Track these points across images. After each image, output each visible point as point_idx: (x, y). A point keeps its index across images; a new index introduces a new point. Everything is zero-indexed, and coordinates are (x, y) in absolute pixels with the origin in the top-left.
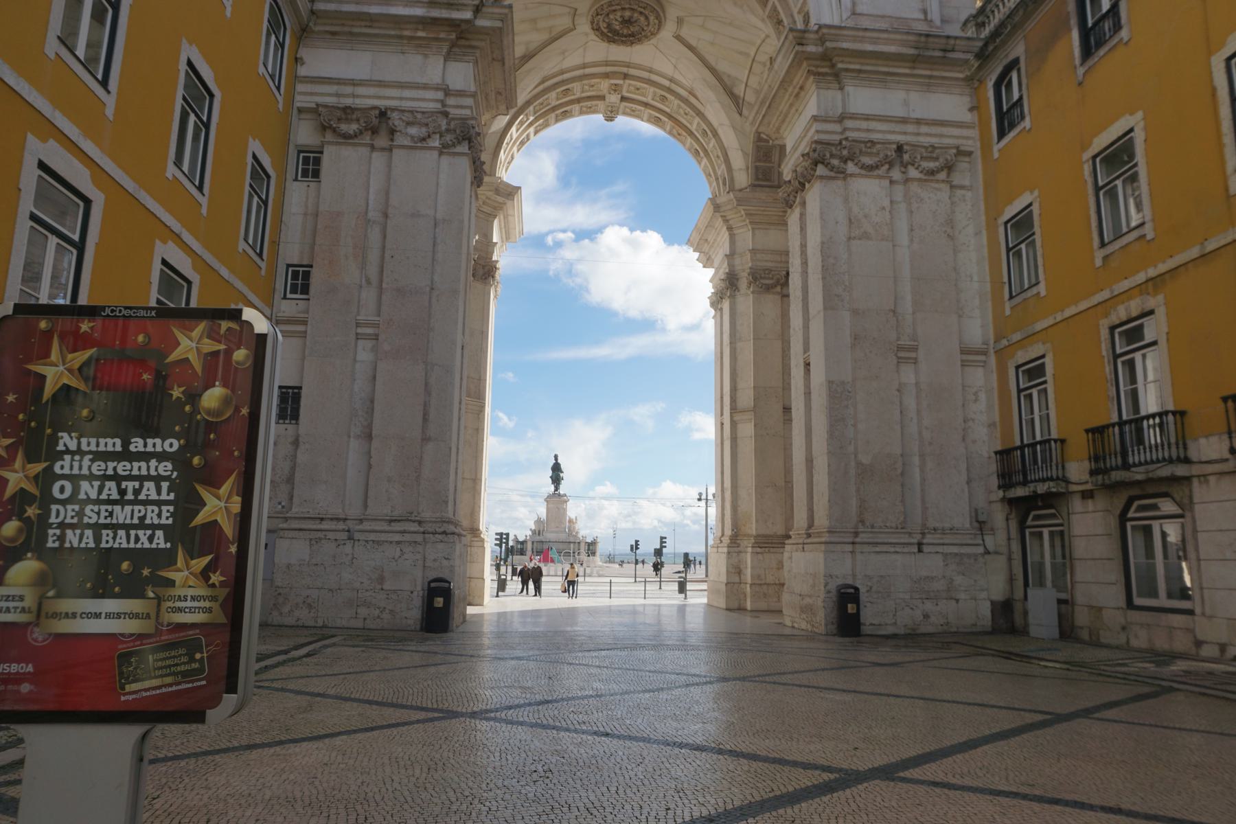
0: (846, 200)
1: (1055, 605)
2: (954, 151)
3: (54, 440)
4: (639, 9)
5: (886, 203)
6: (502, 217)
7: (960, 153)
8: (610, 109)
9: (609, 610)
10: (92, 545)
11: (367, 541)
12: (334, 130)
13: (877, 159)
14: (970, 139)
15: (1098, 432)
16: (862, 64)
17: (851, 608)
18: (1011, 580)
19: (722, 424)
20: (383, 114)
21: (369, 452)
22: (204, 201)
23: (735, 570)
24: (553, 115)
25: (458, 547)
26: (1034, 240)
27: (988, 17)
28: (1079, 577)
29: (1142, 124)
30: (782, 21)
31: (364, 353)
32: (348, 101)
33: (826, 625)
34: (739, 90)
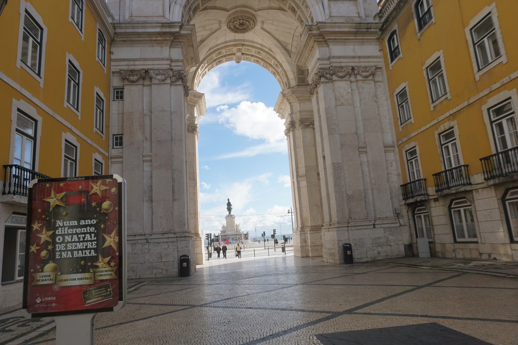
0: (334, 91)
1: (428, 244)
2: (375, 68)
3: (56, 223)
4: (246, 19)
5: (350, 90)
6: (198, 106)
7: (377, 68)
8: (238, 58)
9: (254, 262)
10: (71, 256)
11: (154, 243)
12: (128, 80)
13: (344, 73)
14: (380, 62)
15: (437, 175)
16: (335, 36)
17: (349, 253)
18: (411, 235)
19: (294, 182)
20: (147, 71)
21: (152, 207)
22: (79, 114)
23: (304, 241)
24: (215, 63)
25: (190, 242)
26: (408, 101)
27: (383, 14)
28: (436, 232)
29: (443, 55)
30: (303, 21)
31: (147, 168)
32: (132, 68)
33: (340, 260)
34: (289, 47)
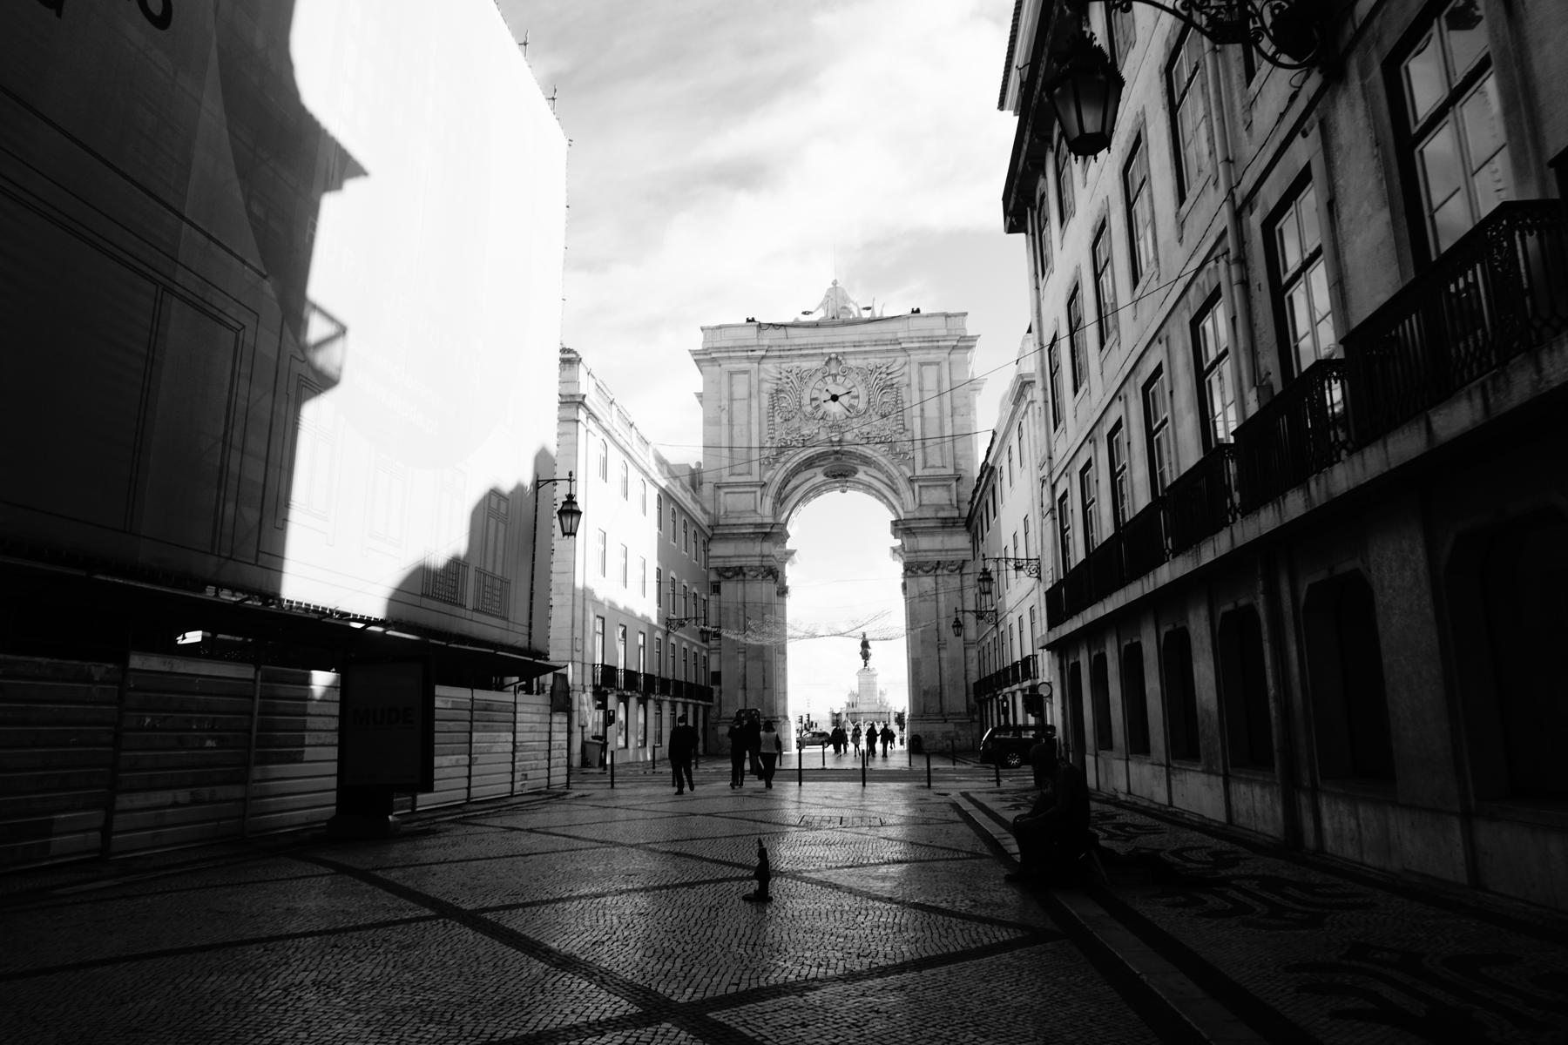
0: (918, 586)
5: (934, 585)
7: (964, 561)
20: (741, 568)
25: (778, 726)
31: (741, 659)
32: (728, 565)
